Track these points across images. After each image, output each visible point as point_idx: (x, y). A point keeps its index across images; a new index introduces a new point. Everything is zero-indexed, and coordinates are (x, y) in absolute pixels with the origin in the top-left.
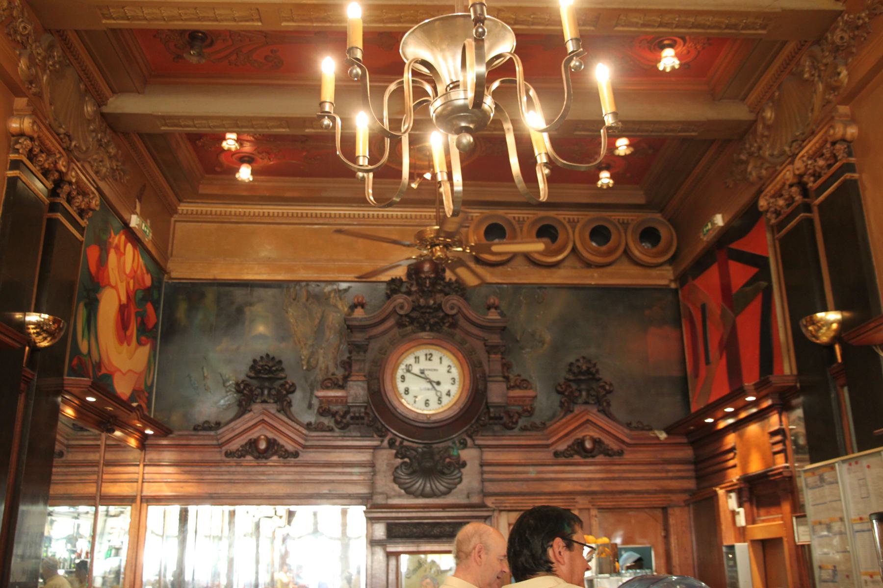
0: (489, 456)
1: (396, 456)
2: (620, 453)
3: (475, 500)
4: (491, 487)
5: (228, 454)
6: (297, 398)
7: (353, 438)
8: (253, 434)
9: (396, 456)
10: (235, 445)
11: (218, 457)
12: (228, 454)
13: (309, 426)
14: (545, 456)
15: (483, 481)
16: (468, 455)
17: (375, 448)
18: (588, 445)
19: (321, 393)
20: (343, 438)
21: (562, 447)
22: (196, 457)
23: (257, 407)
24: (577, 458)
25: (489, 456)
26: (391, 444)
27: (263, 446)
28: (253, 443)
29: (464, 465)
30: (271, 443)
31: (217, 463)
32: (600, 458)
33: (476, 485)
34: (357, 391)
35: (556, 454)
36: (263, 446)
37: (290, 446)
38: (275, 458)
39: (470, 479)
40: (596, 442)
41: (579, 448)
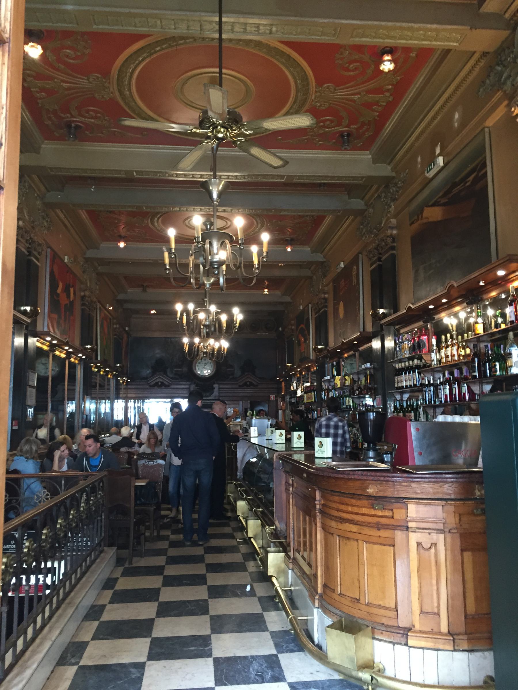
0: (221, 386)
1: (196, 386)
2: (257, 386)
3: (217, 398)
4: (221, 395)
5: (150, 386)
6: (168, 370)
7: (184, 382)
8: (157, 381)
9: (196, 386)
10: (152, 384)
11: (148, 387)
12: (150, 386)
13: (172, 378)
14: (237, 386)
15: (219, 393)
16: (216, 386)
17: (190, 384)
18: (248, 383)
19: (175, 369)
20: (182, 381)
21: (241, 384)
22: (141, 387)
23: (158, 373)
24: (245, 387)
25: (221, 386)
26: (194, 383)
27: (160, 384)
28: (157, 383)
29: (214, 388)
30: (162, 383)
31: (147, 389)
32: (252, 387)
33: (217, 394)
34: (185, 369)
35: (239, 386)
36: (160, 384)
37: (167, 384)
38: (163, 387)
39: (216, 393)
40: (251, 383)
41: (245, 384)
